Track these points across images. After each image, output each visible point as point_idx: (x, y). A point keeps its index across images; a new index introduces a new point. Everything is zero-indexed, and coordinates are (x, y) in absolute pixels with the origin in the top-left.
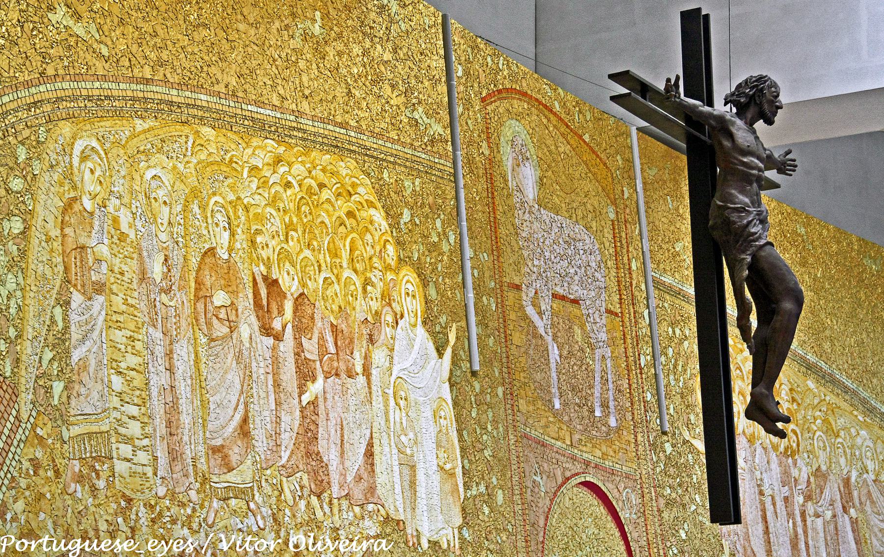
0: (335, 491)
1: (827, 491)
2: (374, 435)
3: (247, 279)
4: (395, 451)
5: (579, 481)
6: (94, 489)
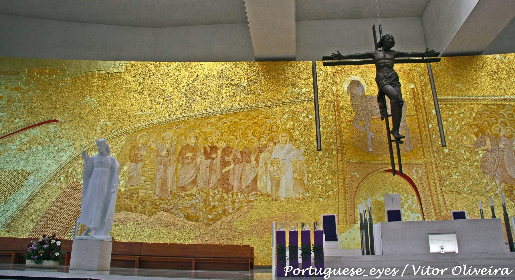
0: (235, 191)
2: (258, 175)
3: (202, 148)
4: (269, 178)
5: (381, 170)
6: (131, 200)
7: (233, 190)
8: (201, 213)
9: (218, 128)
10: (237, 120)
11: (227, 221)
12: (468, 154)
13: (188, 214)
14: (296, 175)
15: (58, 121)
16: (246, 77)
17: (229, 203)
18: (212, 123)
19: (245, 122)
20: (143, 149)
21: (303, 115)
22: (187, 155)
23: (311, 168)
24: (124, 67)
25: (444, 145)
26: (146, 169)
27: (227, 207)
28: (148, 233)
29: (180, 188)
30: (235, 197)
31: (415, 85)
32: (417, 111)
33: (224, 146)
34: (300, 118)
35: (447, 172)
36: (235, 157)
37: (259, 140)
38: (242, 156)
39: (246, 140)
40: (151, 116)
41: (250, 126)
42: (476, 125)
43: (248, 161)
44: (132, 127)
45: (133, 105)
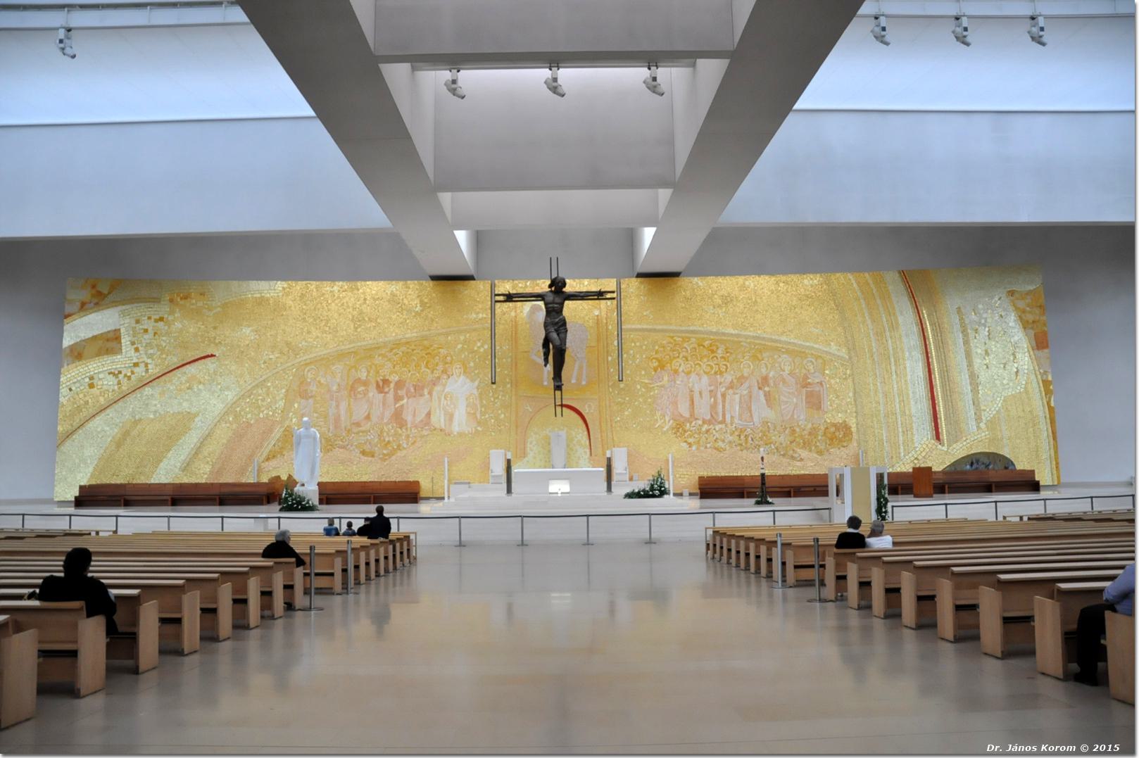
0: (409, 426)
1: (746, 385)
3: (373, 381)
4: (443, 412)
7: (407, 425)
8: (376, 449)
9: (390, 359)
10: (410, 350)
11: (403, 455)
12: (643, 390)
13: (364, 450)
14: (469, 409)
15: (215, 356)
16: (417, 301)
17: (403, 437)
18: (382, 354)
19: (418, 353)
20: (312, 384)
21: (479, 344)
22: (359, 390)
23: (484, 402)
24: (281, 289)
25: (621, 379)
26: (318, 405)
27: (401, 442)
28: (325, 470)
29: (354, 424)
30: (409, 432)
31: (601, 313)
32: (598, 340)
33: (397, 378)
34: (476, 349)
35: (619, 408)
36: (408, 391)
37: (432, 372)
38: (415, 389)
39: (419, 373)
40: (317, 347)
41: (422, 357)
42: (656, 359)
43: (422, 395)
44: (298, 361)
45: (297, 335)
